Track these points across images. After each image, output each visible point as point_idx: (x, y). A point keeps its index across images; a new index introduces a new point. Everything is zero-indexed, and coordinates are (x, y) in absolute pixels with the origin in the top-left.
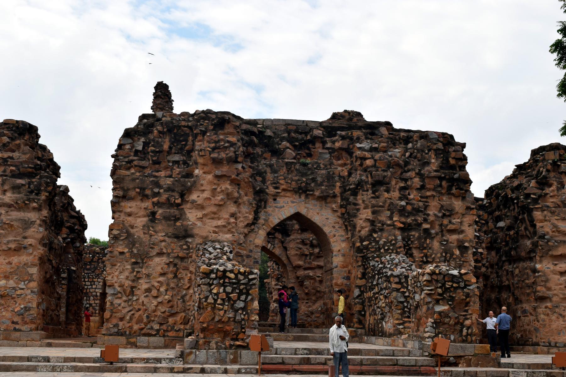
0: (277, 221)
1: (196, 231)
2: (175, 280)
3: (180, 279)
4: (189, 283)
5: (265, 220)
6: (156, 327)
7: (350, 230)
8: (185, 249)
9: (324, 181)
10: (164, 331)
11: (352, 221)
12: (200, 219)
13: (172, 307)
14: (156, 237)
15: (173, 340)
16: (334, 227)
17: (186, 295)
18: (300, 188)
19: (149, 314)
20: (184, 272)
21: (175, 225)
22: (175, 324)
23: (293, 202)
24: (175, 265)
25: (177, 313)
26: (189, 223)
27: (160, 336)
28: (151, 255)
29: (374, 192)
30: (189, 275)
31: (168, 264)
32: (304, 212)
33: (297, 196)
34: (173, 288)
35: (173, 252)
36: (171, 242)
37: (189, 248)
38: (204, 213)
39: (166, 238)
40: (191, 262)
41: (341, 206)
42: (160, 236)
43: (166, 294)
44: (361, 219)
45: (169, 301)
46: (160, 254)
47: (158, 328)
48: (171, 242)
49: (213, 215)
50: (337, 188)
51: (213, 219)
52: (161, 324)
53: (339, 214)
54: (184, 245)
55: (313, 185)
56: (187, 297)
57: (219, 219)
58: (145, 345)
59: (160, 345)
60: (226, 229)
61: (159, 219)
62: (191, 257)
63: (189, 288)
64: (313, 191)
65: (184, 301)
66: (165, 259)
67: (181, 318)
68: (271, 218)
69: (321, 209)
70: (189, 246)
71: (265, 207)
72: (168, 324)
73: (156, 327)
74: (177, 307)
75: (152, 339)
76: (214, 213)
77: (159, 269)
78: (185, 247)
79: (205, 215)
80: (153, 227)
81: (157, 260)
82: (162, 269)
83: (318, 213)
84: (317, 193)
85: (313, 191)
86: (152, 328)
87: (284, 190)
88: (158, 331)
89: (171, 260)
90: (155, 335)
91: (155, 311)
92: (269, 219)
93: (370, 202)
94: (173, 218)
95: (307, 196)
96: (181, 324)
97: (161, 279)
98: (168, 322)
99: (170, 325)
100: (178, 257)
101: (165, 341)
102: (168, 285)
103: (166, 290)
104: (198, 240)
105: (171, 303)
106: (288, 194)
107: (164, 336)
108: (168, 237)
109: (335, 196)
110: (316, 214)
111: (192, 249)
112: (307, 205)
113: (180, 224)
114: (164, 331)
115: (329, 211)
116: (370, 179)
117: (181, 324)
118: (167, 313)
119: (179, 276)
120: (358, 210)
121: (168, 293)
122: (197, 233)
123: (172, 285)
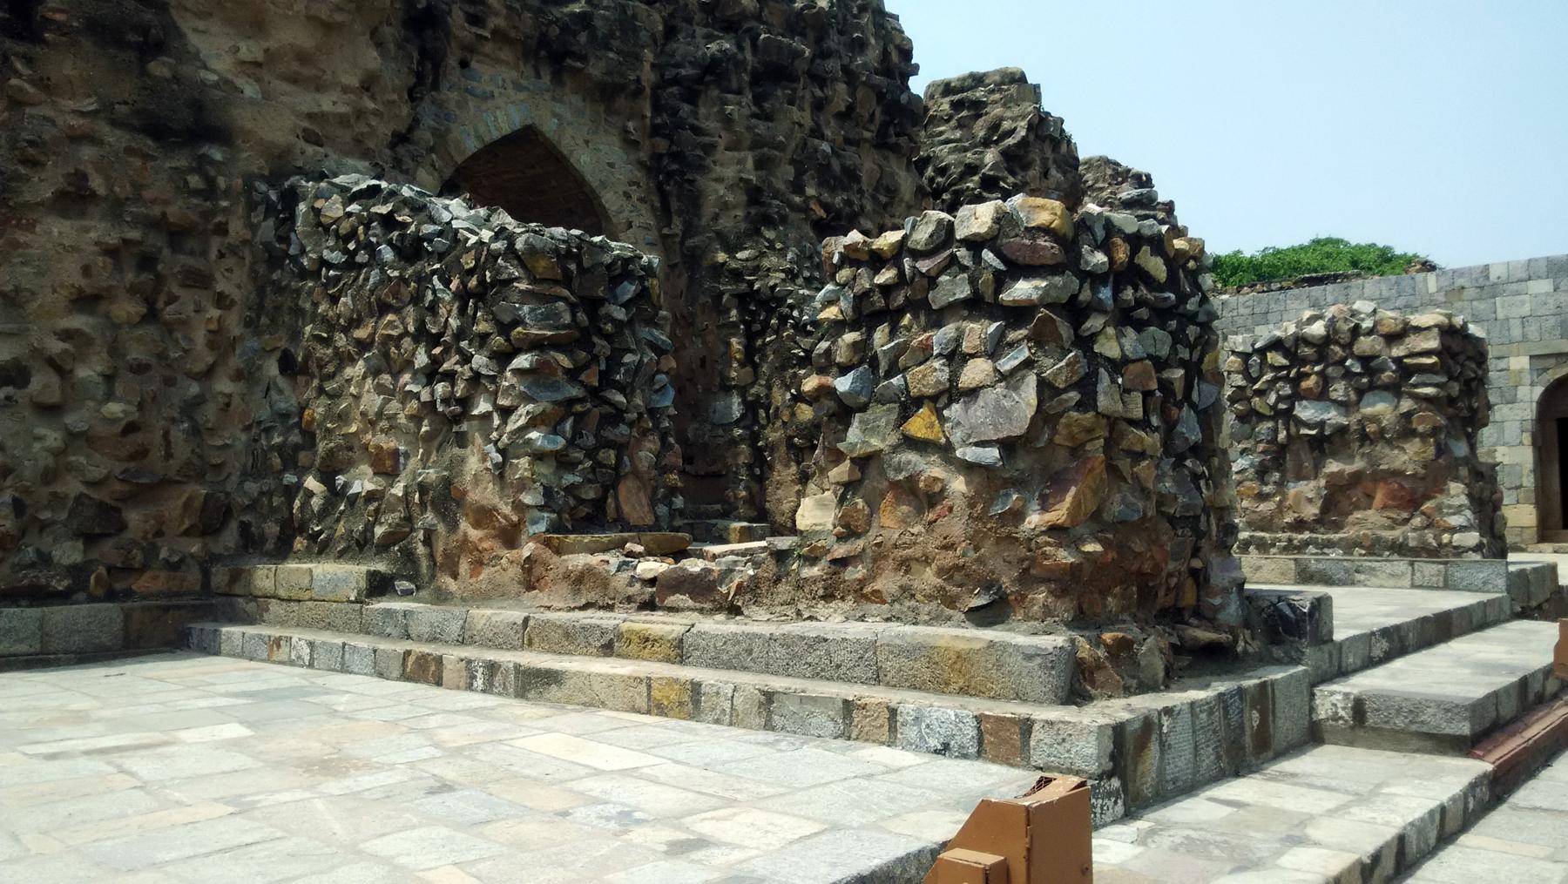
0: (472, 146)
1: (243, 118)
2: (150, 331)
3: (169, 328)
4: (211, 345)
5: (434, 131)
6: (69, 553)
7: (680, 213)
8: (196, 193)
9: (612, 35)
10: (110, 569)
11: (691, 182)
12: (253, 68)
13: (141, 453)
14: (47, 111)
15: (166, 609)
16: (627, 196)
17: (198, 402)
18: (543, 41)
19: (26, 491)
20: (187, 300)
21: (144, 73)
22: (159, 533)
23: (518, 87)
24: (147, 262)
25: (165, 483)
26: (203, 74)
27: (92, 599)
28: (27, 197)
29: (758, 100)
30: (214, 313)
31: (111, 252)
32: (549, 126)
33: (529, 71)
34: (140, 369)
35: (138, 199)
36: (129, 151)
37: (210, 191)
38: (265, 45)
39: (104, 130)
40: (221, 255)
41: (656, 131)
42: (70, 111)
43: (110, 396)
44: (720, 180)
45: (131, 428)
46: (75, 199)
47: (77, 557)
48: (129, 151)
49: (295, 66)
50: (647, 67)
51: (294, 80)
52: (90, 539)
53: (644, 155)
54: (192, 171)
55: (583, 38)
56: (209, 413)
57: (319, 87)
58: (23, 648)
59: (105, 639)
60: (345, 135)
61: (60, 28)
62: (222, 230)
63: (209, 373)
64: (584, 58)
65: (196, 431)
66: (98, 230)
67: (187, 506)
68: (456, 132)
69: (596, 133)
70: (211, 182)
71: (435, 86)
72: (128, 535)
73: (69, 553)
74: (169, 455)
75: (59, 614)
76: (303, 58)
77: (70, 273)
78: (195, 181)
79: (271, 57)
80: (29, 61)
81: (58, 228)
82: (86, 271)
83: (587, 142)
84: (595, 70)
85: (584, 58)
86: (45, 559)
87: (498, 34)
88: (78, 573)
89: (134, 234)
90: (64, 597)
91: (49, 476)
92: (448, 130)
93: (749, 128)
94: (133, 38)
95: (557, 79)
96: (186, 533)
97: (78, 322)
98: (122, 527)
99: (134, 543)
100: (157, 224)
101: (127, 616)
102: (115, 350)
103: (109, 378)
104: (250, 160)
105: (138, 438)
106: (506, 54)
107: (111, 596)
108: (114, 123)
109: (638, 92)
110: (581, 142)
111: (227, 194)
112: (558, 108)
113: (166, 73)
114: (110, 569)
115: (615, 140)
116: (749, 56)
117: (186, 533)
118: (119, 487)
119: (169, 313)
120: (710, 148)
121: (119, 388)
122: (249, 125)
123: (136, 354)
